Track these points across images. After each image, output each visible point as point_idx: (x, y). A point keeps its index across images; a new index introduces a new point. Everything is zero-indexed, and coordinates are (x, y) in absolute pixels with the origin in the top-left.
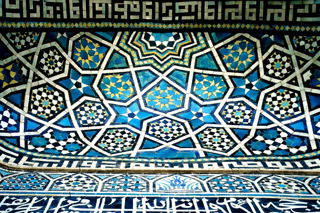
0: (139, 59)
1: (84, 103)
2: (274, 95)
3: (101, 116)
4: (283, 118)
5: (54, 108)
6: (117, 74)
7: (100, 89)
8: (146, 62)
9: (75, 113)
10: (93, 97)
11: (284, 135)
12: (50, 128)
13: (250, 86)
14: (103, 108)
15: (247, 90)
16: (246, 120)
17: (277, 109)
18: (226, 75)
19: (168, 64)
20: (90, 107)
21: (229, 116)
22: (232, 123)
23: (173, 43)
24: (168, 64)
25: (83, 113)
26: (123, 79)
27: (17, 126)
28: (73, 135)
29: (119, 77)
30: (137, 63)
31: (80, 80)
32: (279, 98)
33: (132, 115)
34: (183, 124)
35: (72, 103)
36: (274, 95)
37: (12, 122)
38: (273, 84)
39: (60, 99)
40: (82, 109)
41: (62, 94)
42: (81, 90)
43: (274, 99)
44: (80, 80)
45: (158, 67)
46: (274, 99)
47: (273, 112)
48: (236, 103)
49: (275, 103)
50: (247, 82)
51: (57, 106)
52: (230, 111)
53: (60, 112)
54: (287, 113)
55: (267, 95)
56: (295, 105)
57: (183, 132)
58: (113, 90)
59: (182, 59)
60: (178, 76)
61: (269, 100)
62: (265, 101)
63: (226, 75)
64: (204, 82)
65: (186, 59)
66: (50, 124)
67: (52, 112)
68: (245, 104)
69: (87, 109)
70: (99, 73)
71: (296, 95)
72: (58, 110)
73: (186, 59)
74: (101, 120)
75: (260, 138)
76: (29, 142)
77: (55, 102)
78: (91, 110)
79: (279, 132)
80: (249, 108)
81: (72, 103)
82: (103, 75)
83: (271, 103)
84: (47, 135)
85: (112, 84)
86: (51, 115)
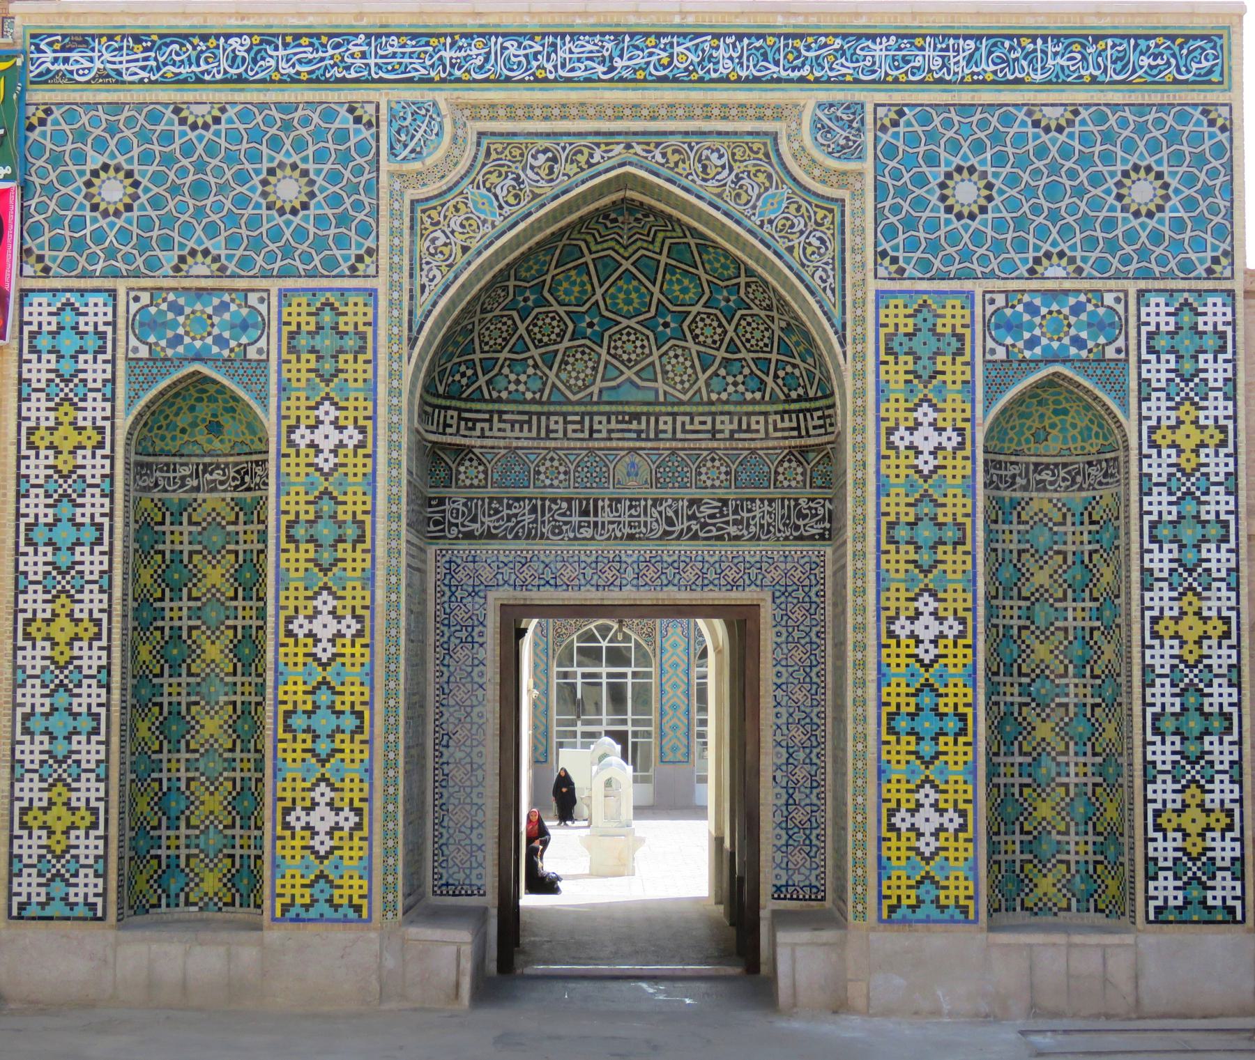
0: (597, 243)
1: (536, 317)
3: (557, 330)
8: (605, 245)
9: (529, 332)
11: (746, 371)
15: (723, 303)
16: (714, 342)
18: (704, 277)
19: (634, 247)
21: (698, 331)
24: (634, 247)
26: (578, 274)
27: (475, 374)
28: (531, 362)
29: (573, 273)
30: (594, 248)
31: (527, 294)
33: (591, 325)
37: (469, 372)
42: (530, 303)
44: (527, 294)
45: (621, 251)
48: (709, 315)
52: (701, 324)
55: (743, 317)
57: (647, 351)
58: (567, 293)
59: (652, 242)
60: (647, 266)
61: (743, 323)
62: (738, 324)
63: (704, 277)
65: (658, 244)
66: (505, 354)
69: (540, 323)
70: (548, 278)
73: (658, 244)
75: (722, 372)
80: (720, 325)
84: (506, 371)
85: (565, 285)
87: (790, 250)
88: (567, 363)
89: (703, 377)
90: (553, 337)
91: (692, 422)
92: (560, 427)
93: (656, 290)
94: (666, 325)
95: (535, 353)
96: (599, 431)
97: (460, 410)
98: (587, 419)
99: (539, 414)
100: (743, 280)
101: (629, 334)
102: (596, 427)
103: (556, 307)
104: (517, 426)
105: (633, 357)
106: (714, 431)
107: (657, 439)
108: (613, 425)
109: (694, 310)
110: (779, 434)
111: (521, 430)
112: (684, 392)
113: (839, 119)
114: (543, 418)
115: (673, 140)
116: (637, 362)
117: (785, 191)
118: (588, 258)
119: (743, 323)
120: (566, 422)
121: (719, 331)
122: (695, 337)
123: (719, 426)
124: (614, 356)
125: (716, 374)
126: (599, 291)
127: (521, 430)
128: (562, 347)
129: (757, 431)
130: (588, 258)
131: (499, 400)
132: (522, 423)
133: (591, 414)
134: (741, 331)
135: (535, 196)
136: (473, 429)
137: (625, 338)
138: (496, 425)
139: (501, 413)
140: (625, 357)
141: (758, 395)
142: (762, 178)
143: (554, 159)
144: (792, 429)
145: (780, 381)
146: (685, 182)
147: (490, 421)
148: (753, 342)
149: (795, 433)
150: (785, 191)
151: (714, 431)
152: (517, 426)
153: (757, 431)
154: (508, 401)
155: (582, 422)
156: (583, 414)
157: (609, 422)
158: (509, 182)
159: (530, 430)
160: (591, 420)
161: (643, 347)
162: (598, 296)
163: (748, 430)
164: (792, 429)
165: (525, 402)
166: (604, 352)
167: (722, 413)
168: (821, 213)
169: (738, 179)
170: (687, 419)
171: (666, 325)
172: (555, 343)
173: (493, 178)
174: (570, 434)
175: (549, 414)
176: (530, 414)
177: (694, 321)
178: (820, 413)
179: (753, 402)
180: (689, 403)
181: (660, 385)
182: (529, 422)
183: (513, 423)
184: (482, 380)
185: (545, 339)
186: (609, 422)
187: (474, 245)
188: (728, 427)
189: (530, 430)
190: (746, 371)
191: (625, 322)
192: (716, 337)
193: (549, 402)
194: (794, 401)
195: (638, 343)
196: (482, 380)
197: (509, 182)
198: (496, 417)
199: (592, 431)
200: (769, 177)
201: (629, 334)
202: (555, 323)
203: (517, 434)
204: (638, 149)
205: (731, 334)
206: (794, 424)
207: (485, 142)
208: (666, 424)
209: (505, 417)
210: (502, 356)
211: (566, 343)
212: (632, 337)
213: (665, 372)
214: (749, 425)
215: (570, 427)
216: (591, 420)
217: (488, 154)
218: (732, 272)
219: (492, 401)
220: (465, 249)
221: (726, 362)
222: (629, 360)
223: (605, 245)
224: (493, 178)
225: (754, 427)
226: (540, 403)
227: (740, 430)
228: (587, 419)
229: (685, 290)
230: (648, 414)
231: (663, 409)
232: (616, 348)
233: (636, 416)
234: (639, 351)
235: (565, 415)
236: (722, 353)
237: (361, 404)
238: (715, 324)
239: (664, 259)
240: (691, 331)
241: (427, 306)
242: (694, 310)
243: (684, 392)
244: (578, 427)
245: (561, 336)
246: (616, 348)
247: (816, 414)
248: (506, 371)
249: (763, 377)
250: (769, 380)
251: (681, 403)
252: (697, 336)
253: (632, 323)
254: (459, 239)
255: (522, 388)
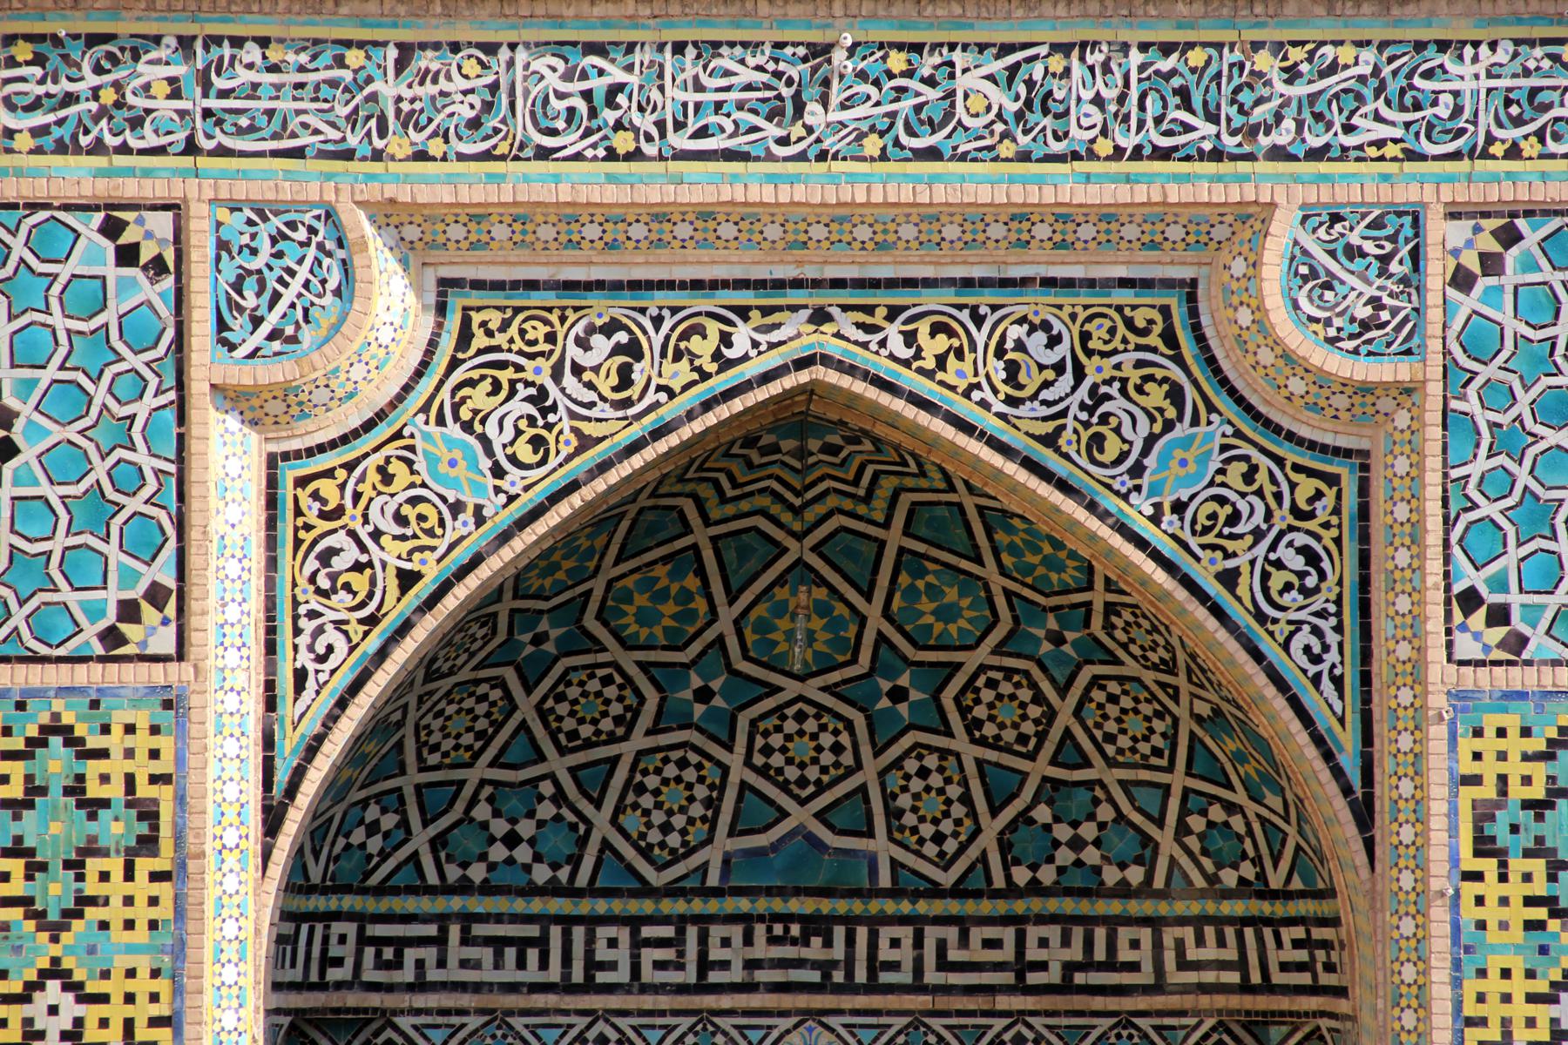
0: (724, 500)
1: (563, 679)
2: (1114, 688)
3: (616, 709)
4: (1120, 759)
5: (482, 724)
6: (654, 562)
7: (605, 624)
8: (745, 506)
9: (543, 714)
10: (588, 651)
11: (1105, 813)
12: (483, 783)
13: (1057, 639)
14: (618, 679)
15: (1046, 647)
16: (1023, 739)
17: (1111, 727)
19: (820, 509)
20: (582, 684)
21: (980, 712)
22: (982, 742)
23: (841, 448)
24: (820, 509)
25: (563, 708)
26: (675, 575)
27: (404, 824)
28: (547, 788)
29: (660, 571)
30: (715, 514)
31: (543, 625)
32: (1126, 702)
33: (704, 695)
34: (850, 726)
35: (529, 690)
36: (1114, 688)
37: (389, 821)
38: (1117, 662)
39: (496, 694)
40: (560, 698)
41: (500, 683)
42: (549, 647)
43: (1113, 699)
44: (543, 625)
45: (786, 517)
46: (1113, 699)
47: (1098, 734)
48: (1009, 673)
49: (1113, 711)
50: (1052, 623)
51: (488, 715)
52: (987, 695)
53: (498, 726)
54: (1133, 750)
55: (1096, 682)
56: (1157, 741)
57: (847, 759)
58: (644, 618)
59: (868, 498)
60: (850, 553)
61: (1098, 696)
62: (1085, 698)
63: (998, 583)
64: (929, 586)
66: (481, 770)
67: (480, 735)
68: (1033, 685)
69: (573, 692)
70: (598, 586)
71: (1169, 719)
72: (492, 723)
74: (618, 720)
75: (1043, 814)
76: (443, 855)
77: (482, 709)
78: (585, 694)
79: (1096, 802)
80: (1039, 698)
81: (529, 690)
82: (610, 584)
83: (1100, 706)
84: (482, 812)
85: (641, 600)
86: (478, 745)
87: (1229, 579)
88: (641, 789)
89: (992, 828)
90: (606, 725)
91: (964, 941)
92: (622, 955)
93: (873, 611)
94: (898, 695)
95: (559, 765)
96: (725, 965)
97: (361, 918)
98: (692, 932)
99: (567, 921)
100: (1098, 597)
101: (801, 717)
102: (716, 954)
103: (615, 652)
104: (510, 953)
105: (812, 773)
106: (1022, 966)
107: (873, 987)
108: (761, 950)
109: (972, 660)
110: (1191, 977)
111: (521, 964)
112: (945, 862)
113: (1353, 252)
114: (579, 932)
115: (931, 300)
116: (821, 788)
117: (1215, 431)
118: (701, 536)
119: (1098, 696)
120: (638, 944)
121: (1035, 711)
122: (973, 725)
123: (1033, 953)
124: (763, 771)
125: (1024, 817)
126: (727, 615)
127: (521, 964)
128: (627, 749)
129: (1134, 967)
130: (701, 536)
131: (464, 887)
132: (523, 944)
133: (703, 920)
134: (1091, 714)
135: (586, 443)
136: (397, 964)
137: (790, 726)
138: (455, 951)
139: (468, 919)
140: (792, 773)
141: (1135, 875)
142: (1156, 396)
143: (633, 350)
144: (1223, 965)
145: (1193, 843)
146: (964, 408)
147: (441, 941)
148: (1123, 741)
149: (1233, 977)
150: (1215, 431)
151: (1022, 966)
152: (510, 953)
153: (1134, 967)
154: (487, 889)
155: (677, 942)
156: (681, 922)
157: (748, 940)
158: (519, 407)
159: (544, 964)
160: (703, 939)
161: (837, 749)
162: (724, 625)
163: (1111, 965)
164: (1223, 965)
165: (532, 891)
166: (735, 761)
167: (1041, 920)
168: (1307, 486)
169: (1098, 398)
170: (952, 933)
171: (898, 695)
172: (612, 739)
173: (479, 398)
174: (648, 975)
175: (592, 922)
176: (544, 920)
177: (969, 685)
178: (1299, 932)
179: (1124, 891)
180: (958, 892)
181: (880, 845)
182: (542, 943)
183: (498, 943)
184: (420, 839)
185: (586, 731)
186: (748, 940)
187: (432, 572)
188: (1057, 956)
189: (544, 964)
190: (1105, 813)
191: (792, 688)
192: (1028, 728)
193: (592, 891)
194: (1227, 894)
195: (826, 740)
196: (420, 839)
197: (519, 407)
198: (455, 931)
199: (704, 965)
200: (1176, 395)
201: (801, 717)
202: (611, 692)
203: (510, 974)
204: (845, 323)
205: (1065, 718)
206: (1231, 954)
207: (456, 303)
208: (896, 946)
209: (479, 930)
210: (473, 776)
211: (639, 741)
212: (811, 726)
213: (893, 814)
214: (1111, 947)
215: (649, 955)
216: (703, 939)
217: (465, 338)
218: (1070, 576)
219: (447, 890)
220: (407, 579)
221: (1052, 789)
222: (802, 782)
223: (745, 506)
224: (479, 398)
225: (1125, 955)
226: (571, 892)
227: (1088, 965)
228: (692, 932)
229: (947, 613)
230: (850, 921)
231: (890, 907)
232: (767, 751)
233: (817, 926)
234: (827, 758)
235: (635, 922)
236: (1041, 767)
237: (142, 985)
238: (1025, 694)
239: (894, 538)
240: (964, 711)
241: (311, 726)
242: (972, 660)
243: (945, 862)
244: (667, 954)
245: (627, 722)
246: (767, 751)
247: (1288, 934)
248: (482, 812)
249: (1151, 829)
250: (1165, 838)
251: (935, 891)
252: (979, 724)
253: (812, 689)
254: (391, 554)
255: (523, 854)
